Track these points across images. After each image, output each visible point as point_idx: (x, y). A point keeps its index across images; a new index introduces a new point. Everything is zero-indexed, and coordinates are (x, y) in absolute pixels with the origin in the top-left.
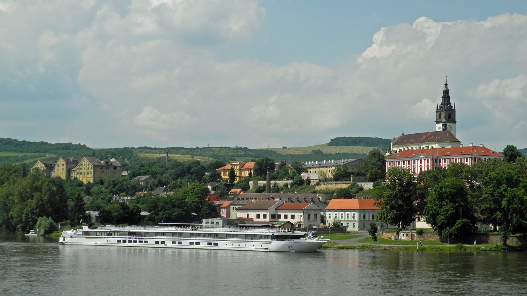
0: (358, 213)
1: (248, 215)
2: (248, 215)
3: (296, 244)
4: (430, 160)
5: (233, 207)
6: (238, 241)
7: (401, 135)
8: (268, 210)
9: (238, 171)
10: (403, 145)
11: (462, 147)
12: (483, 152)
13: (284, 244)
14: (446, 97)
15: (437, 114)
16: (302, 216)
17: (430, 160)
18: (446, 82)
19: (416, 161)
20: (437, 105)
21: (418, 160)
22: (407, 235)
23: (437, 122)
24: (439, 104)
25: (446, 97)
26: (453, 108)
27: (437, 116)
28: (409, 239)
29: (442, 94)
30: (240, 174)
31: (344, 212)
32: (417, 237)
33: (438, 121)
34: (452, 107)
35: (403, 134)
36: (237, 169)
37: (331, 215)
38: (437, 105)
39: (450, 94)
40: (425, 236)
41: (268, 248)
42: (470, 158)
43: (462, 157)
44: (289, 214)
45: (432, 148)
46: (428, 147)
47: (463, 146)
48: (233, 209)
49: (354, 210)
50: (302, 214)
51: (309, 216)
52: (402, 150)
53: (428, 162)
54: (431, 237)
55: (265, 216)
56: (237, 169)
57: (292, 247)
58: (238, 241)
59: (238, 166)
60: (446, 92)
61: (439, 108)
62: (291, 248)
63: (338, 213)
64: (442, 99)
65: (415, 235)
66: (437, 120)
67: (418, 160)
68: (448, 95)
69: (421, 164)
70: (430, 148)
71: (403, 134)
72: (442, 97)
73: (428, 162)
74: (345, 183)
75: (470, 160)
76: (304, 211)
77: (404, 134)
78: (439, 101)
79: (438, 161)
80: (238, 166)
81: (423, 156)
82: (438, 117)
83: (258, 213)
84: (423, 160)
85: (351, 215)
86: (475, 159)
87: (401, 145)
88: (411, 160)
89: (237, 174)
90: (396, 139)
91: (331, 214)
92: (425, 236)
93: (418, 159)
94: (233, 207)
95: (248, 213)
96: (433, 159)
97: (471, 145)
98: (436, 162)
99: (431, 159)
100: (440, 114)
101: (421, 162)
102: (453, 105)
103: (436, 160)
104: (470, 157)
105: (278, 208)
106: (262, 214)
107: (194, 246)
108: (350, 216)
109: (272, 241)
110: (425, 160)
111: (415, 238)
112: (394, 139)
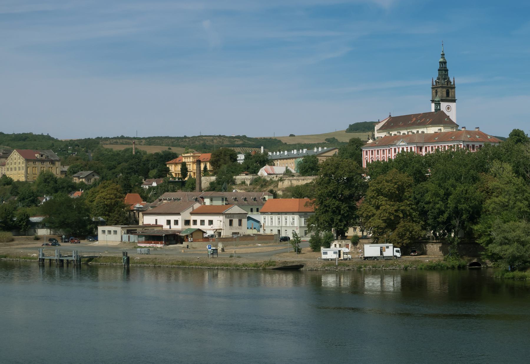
1: (156, 220)
2: (156, 220)
14: (443, 69)
15: (432, 91)
18: (443, 51)
20: (433, 79)
25: (443, 69)
26: (452, 83)
27: (432, 93)
29: (438, 66)
35: (390, 116)
38: (433, 79)
39: (448, 66)
49: (293, 213)
55: (176, 222)
61: (434, 83)
64: (439, 73)
65: (350, 245)
71: (390, 116)
72: (439, 70)
96: (417, 147)
102: (451, 80)
106: (172, 218)
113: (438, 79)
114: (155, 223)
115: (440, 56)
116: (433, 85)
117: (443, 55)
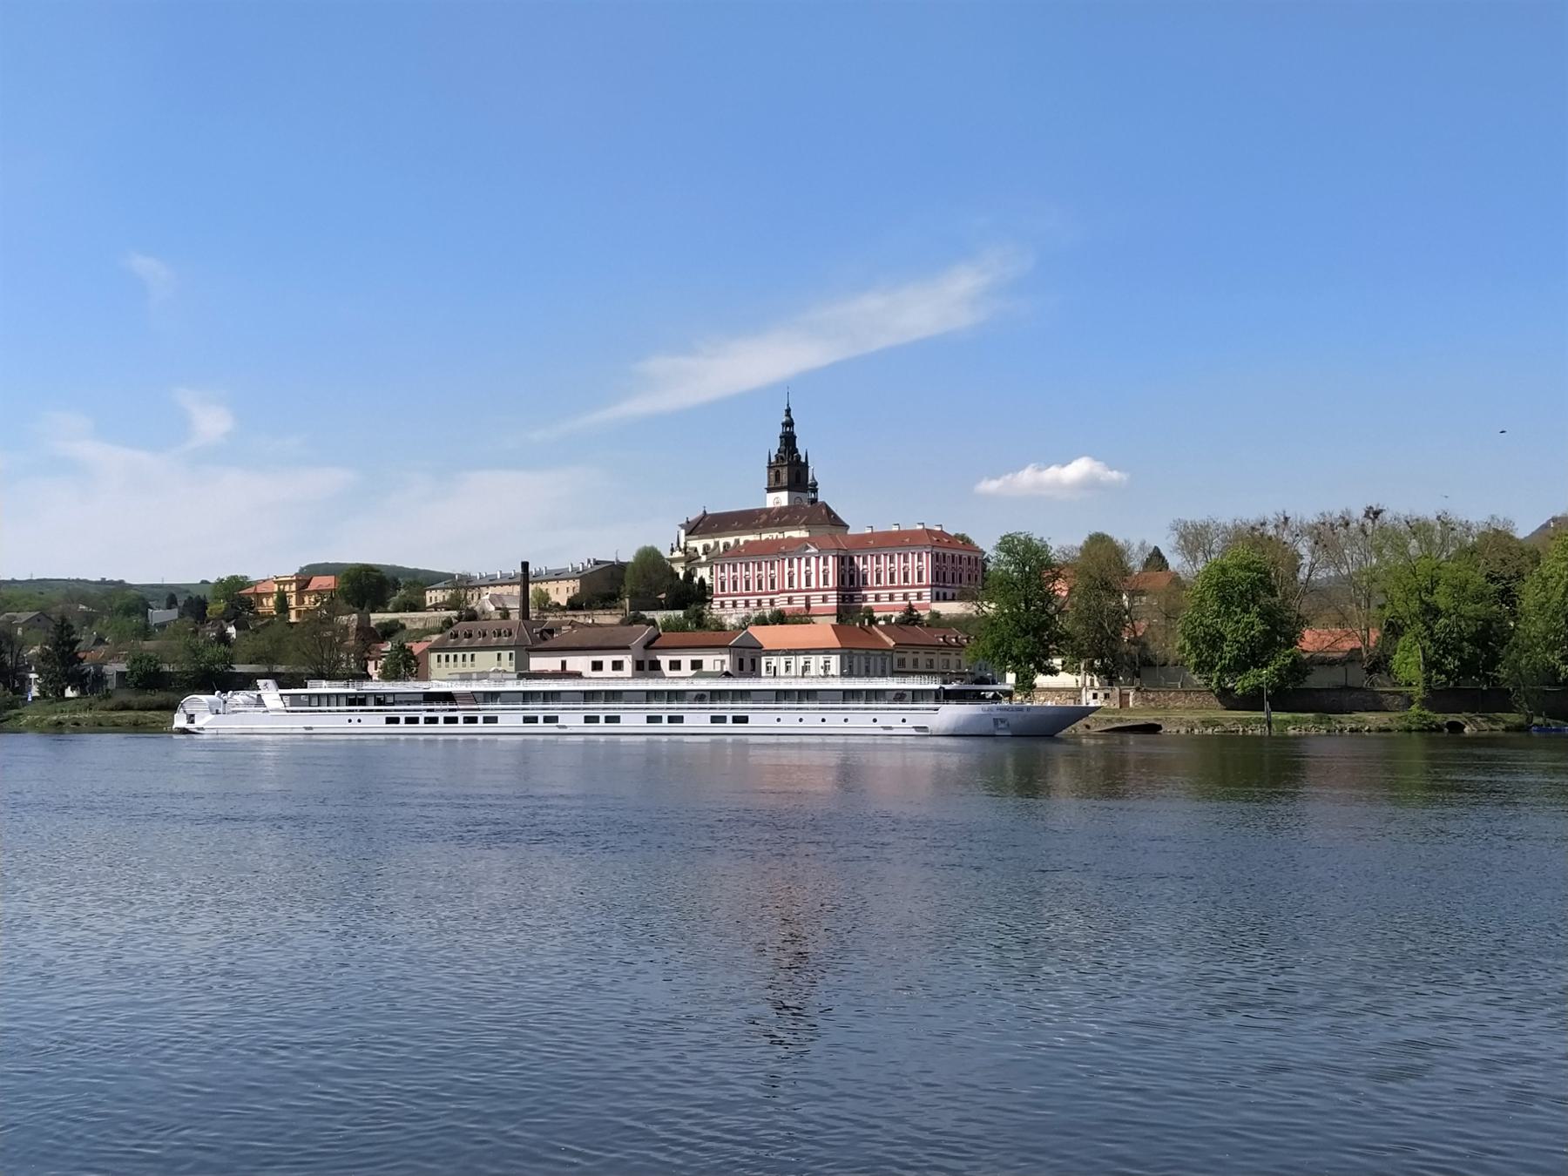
0: (839, 656)
1: (564, 664)
2: (564, 664)
3: (1020, 712)
4: (830, 558)
5: (439, 656)
6: (820, 709)
7: (701, 513)
8: (628, 648)
9: (294, 597)
10: (714, 534)
11: (899, 530)
12: (935, 539)
13: (982, 712)
14: (789, 440)
15: (769, 472)
16: (728, 661)
17: (830, 558)
19: (795, 561)
21: (799, 559)
22: (1106, 696)
23: (770, 490)
24: (775, 452)
25: (789, 440)
26: (803, 460)
27: (769, 477)
28: (1112, 705)
29: (779, 430)
30: (300, 601)
31: (796, 654)
32: (1135, 699)
33: (772, 486)
34: (799, 457)
35: (705, 512)
36: (292, 592)
37: (793, 664)
39: (797, 430)
40: (1162, 695)
41: (925, 727)
42: (927, 553)
43: (906, 552)
44: (686, 660)
45: (726, 545)
46: (717, 544)
47: (901, 529)
48: (439, 660)
49: (827, 651)
50: (726, 657)
51: (741, 661)
52: (732, 545)
53: (825, 563)
54: (1177, 697)
55: (617, 666)
56: (292, 592)
57: (1003, 721)
58: (820, 709)
59: (294, 584)
60: (789, 424)
61: (773, 460)
62: (1002, 726)
63: (814, 657)
64: (781, 442)
65: (1131, 694)
66: (769, 485)
67: (799, 559)
68: (793, 432)
69: (808, 568)
70: (741, 543)
71: (705, 512)
73: (825, 563)
74: (611, 614)
75: (927, 556)
76: (732, 650)
77: (708, 512)
78: (775, 445)
79: (847, 561)
80: (294, 584)
81: (813, 550)
82: (773, 478)
83: (598, 658)
84: (813, 560)
85: (817, 662)
86: (937, 554)
87: (710, 536)
88: (784, 559)
89: (293, 602)
90: (692, 521)
91: (793, 661)
92: (1162, 695)
93: (783, 557)
94: (439, 656)
95: (564, 658)
96: (838, 556)
97: (920, 527)
98: (843, 563)
99: (833, 556)
100: (778, 471)
101: (808, 563)
102: (802, 453)
103: (843, 558)
104: (929, 550)
105: (653, 645)
106: (607, 660)
107: (665, 726)
108: (812, 665)
109: (938, 706)
110: (818, 558)
111: (1131, 704)
112: (688, 522)
113: (779, 451)
114: (560, 668)
115: (784, 413)
116: (770, 462)
117: (788, 411)
